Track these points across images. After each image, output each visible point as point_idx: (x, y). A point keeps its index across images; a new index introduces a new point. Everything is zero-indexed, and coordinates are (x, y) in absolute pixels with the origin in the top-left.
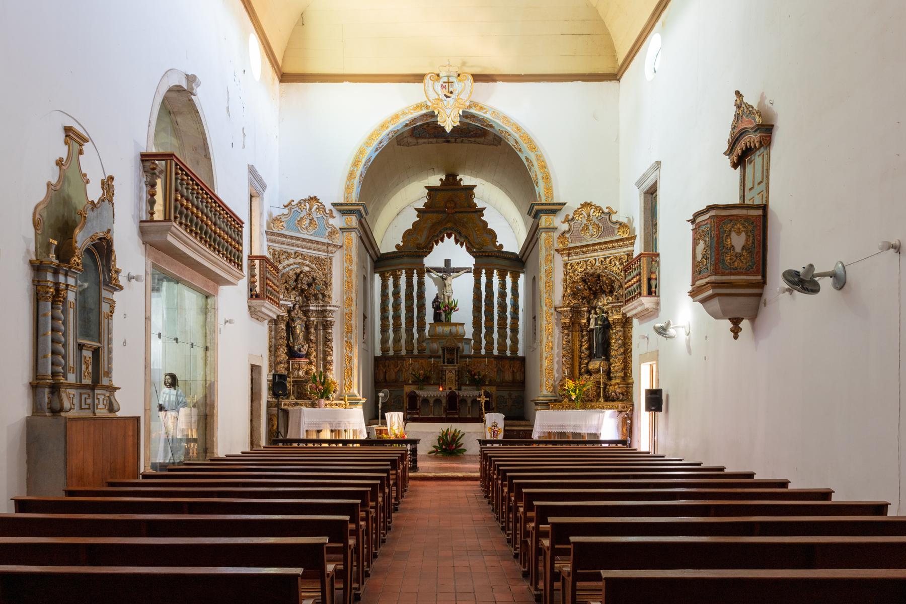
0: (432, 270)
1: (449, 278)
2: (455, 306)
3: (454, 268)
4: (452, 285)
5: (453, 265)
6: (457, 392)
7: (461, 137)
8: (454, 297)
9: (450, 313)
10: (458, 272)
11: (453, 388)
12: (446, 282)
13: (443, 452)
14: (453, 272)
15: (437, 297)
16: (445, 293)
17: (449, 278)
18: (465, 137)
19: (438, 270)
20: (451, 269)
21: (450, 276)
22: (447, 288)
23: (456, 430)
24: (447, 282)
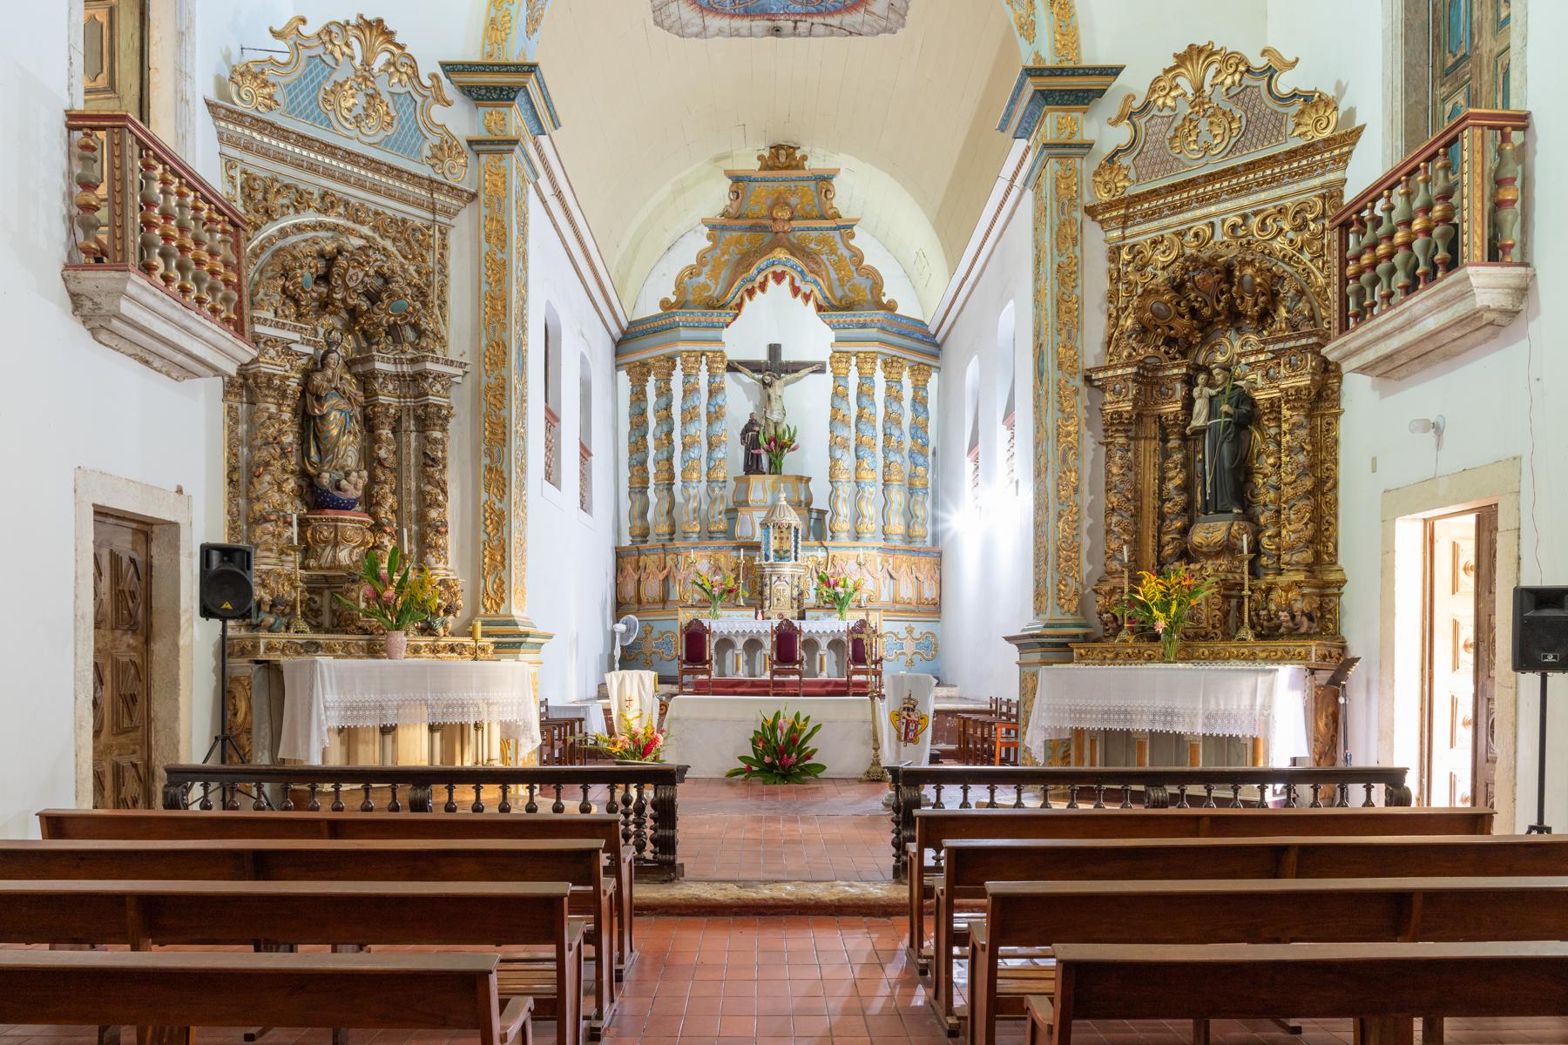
0: (740, 367)
1: (777, 383)
2: (792, 440)
3: (788, 363)
4: (784, 398)
5: (787, 356)
6: (796, 623)
7: (807, 14)
8: (790, 421)
9: (779, 456)
10: (797, 371)
11: (788, 616)
12: (771, 391)
13: (766, 771)
14: (787, 372)
15: (752, 424)
16: (768, 415)
17: (777, 383)
18: (819, 13)
19: (754, 367)
20: (781, 364)
21: (779, 378)
22: (773, 403)
23: (797, 716)
24: (774, 392)
